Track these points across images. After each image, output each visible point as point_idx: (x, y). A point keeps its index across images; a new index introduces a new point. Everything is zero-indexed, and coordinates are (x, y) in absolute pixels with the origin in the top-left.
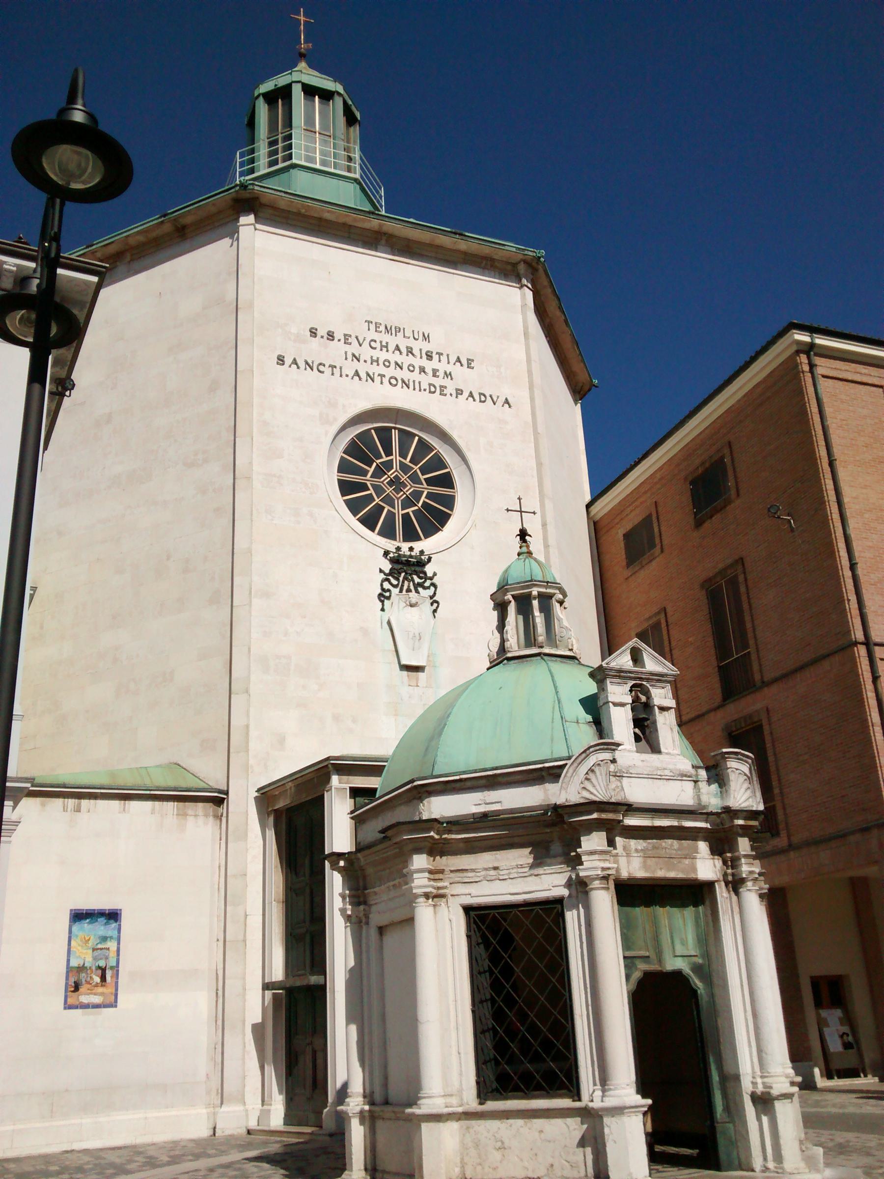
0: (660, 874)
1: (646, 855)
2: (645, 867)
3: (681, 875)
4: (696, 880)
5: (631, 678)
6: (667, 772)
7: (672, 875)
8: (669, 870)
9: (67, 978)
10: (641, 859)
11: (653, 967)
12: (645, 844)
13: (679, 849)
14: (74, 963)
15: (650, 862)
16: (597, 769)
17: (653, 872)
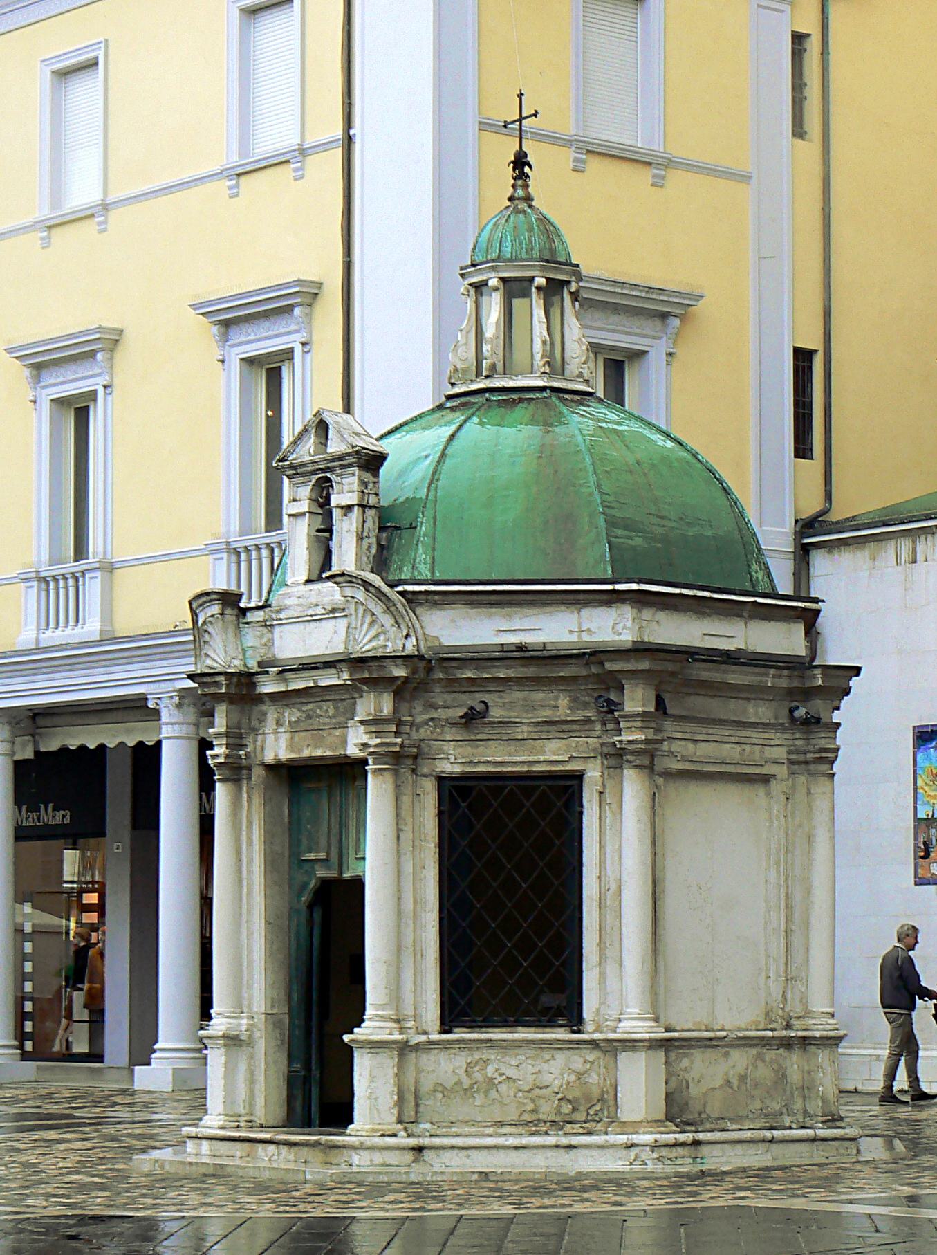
0: (306, 753)
1: (295, 728)
2: (291, 746)
3: (329, 753)
4: (346, 756)
5: (313, 473)
6: (319, 610)
7: (319, 753)
8: (316, 747)
9: (916, 839)
10: (288, 735)
11: (333, 874)
12: (299, 714)
13: (334, 716)
14: (921, 815)
15: (297, 737)
16: (210, 629)
17: (300, 751)
